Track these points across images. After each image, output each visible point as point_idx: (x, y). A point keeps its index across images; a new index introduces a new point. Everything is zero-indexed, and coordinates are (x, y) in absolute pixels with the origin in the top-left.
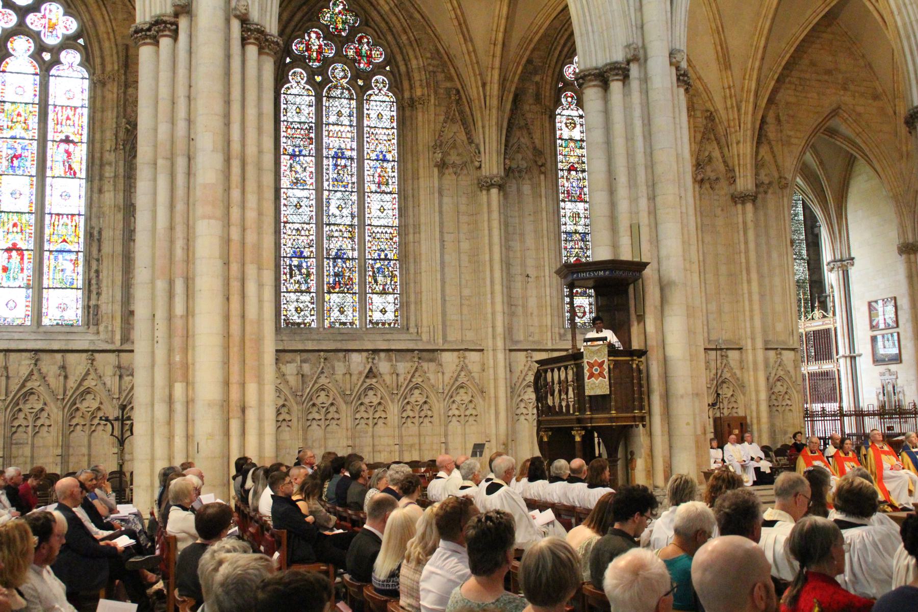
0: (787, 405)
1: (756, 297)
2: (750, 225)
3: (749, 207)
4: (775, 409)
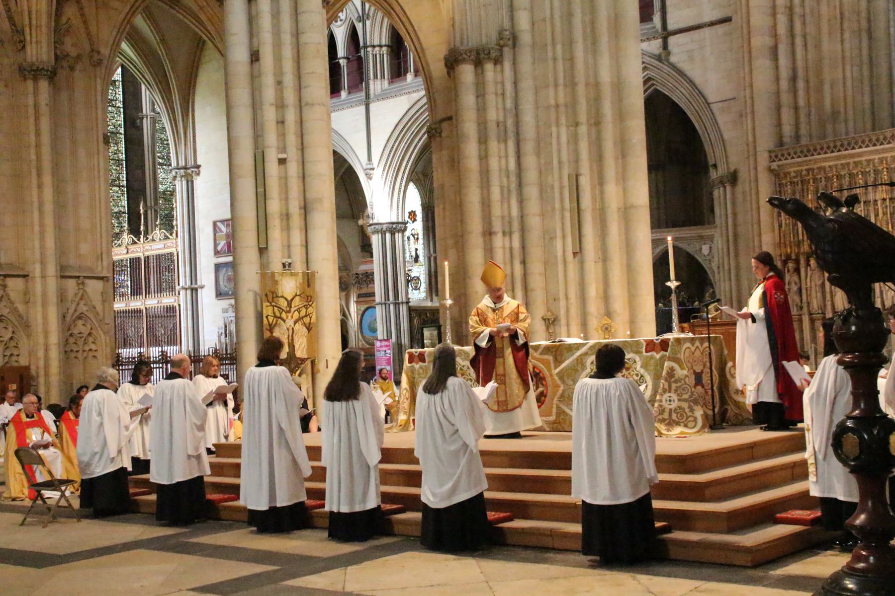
0: (90, 350)
1: (49, 207)
2: (44, 109)
3: (44, 85)
4: (73, 355)
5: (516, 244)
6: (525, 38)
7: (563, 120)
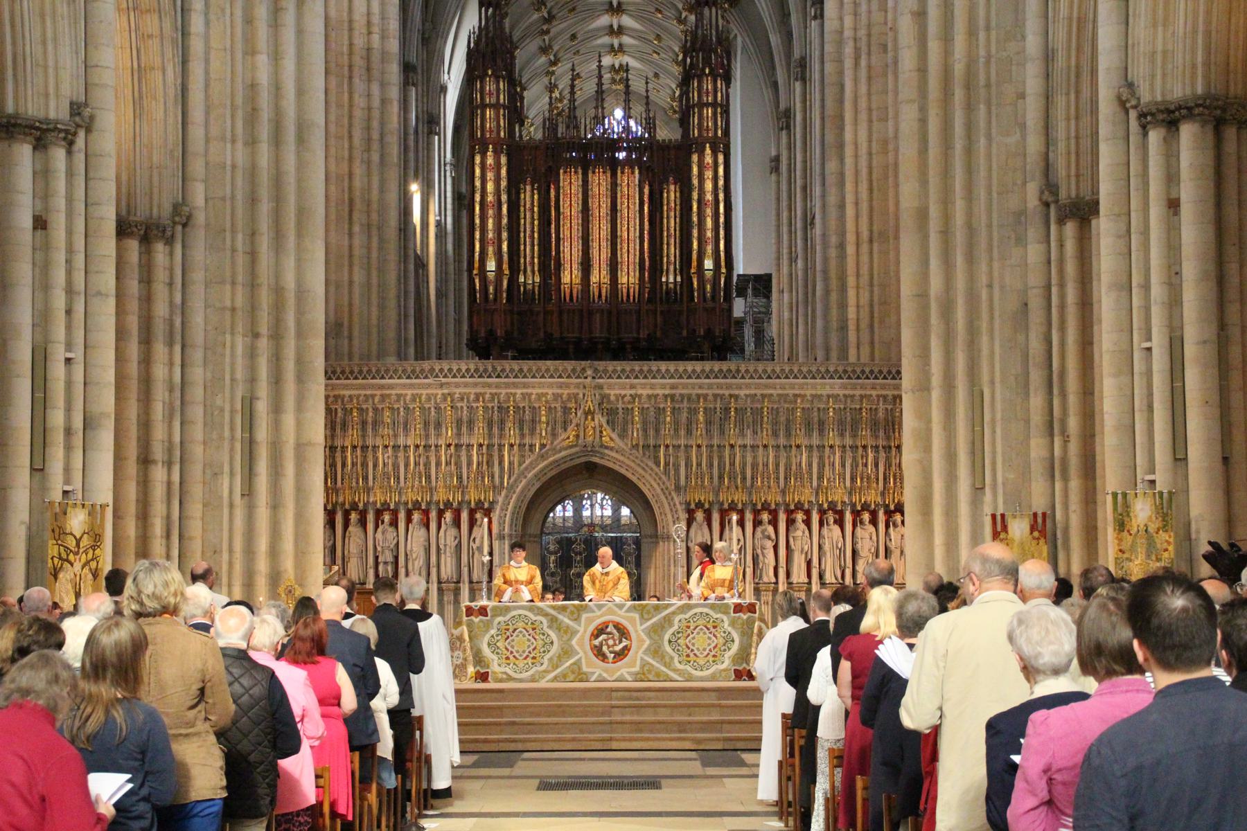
5: (176, 478)
6: (200, 218)
7: (240, 328)
